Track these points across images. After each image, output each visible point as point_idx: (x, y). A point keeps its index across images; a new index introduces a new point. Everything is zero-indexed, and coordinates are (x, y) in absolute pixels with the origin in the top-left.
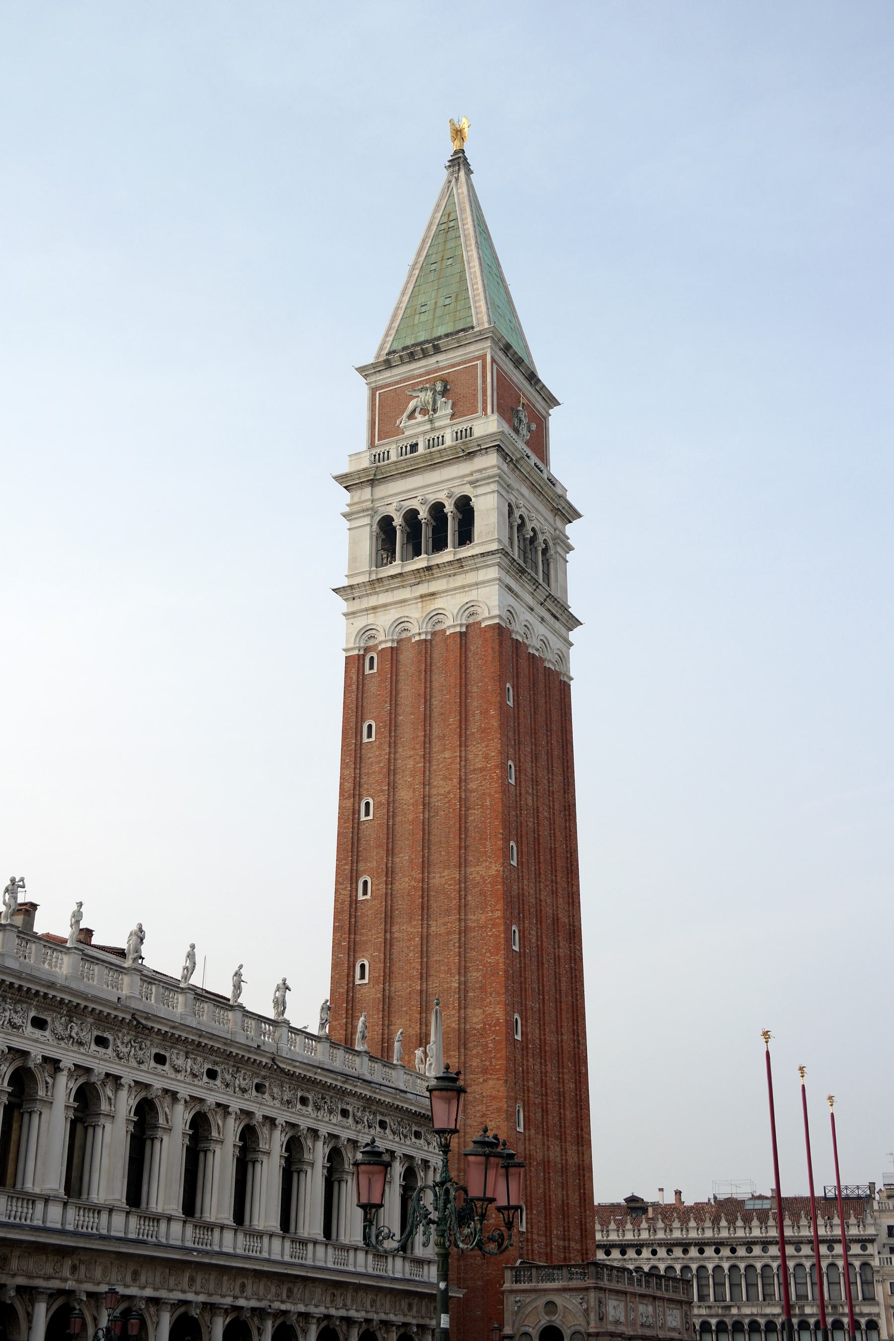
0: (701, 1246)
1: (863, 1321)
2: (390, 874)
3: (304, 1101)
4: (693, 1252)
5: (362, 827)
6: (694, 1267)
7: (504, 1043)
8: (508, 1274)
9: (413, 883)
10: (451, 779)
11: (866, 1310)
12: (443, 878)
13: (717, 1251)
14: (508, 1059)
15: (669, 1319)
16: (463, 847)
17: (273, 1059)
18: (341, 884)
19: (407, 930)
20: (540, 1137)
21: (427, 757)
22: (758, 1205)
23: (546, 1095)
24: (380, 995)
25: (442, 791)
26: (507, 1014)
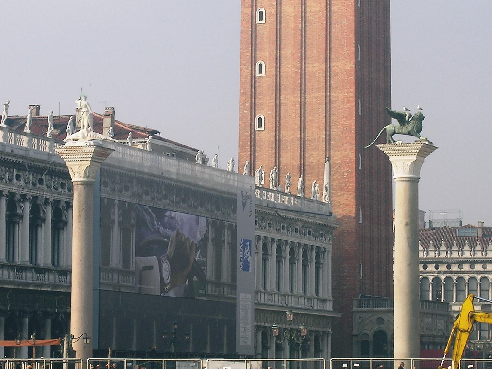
2: (278, 60)
3: (283, 228)
5: (258, 28)
7: (354, 173)
8: (355, 303)
9: (294, 69)
10: (320, 3)
12: (315, 68)
13: (437, 267)
15: (439, 325)
16: (328, 49)
17: (276, 211)
19: (290, 100)
22: (469, 233)
24: (273, 139)
25: (313, 10)
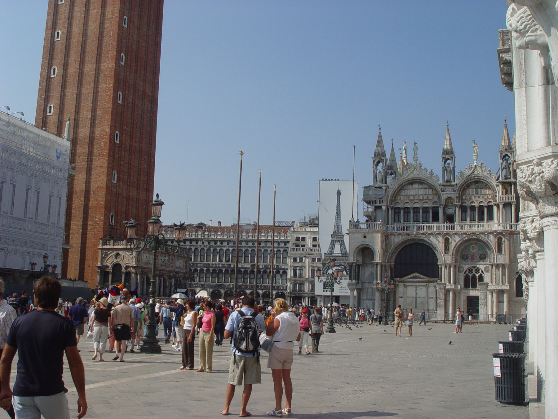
0: (222, 241)
1: (281, 271)
2: (66, 65)
4: (219, 244)
6: (218, 249)
11: (283, 267)
12: (89, 68)
13: (228, 244)
14: (110, 150)
18: (44, 69)
20: (126, 186)
21: (87, 12)
22: (249, 227)
23: (131, 168)
24: (57, 120)
26: (111, 130)
